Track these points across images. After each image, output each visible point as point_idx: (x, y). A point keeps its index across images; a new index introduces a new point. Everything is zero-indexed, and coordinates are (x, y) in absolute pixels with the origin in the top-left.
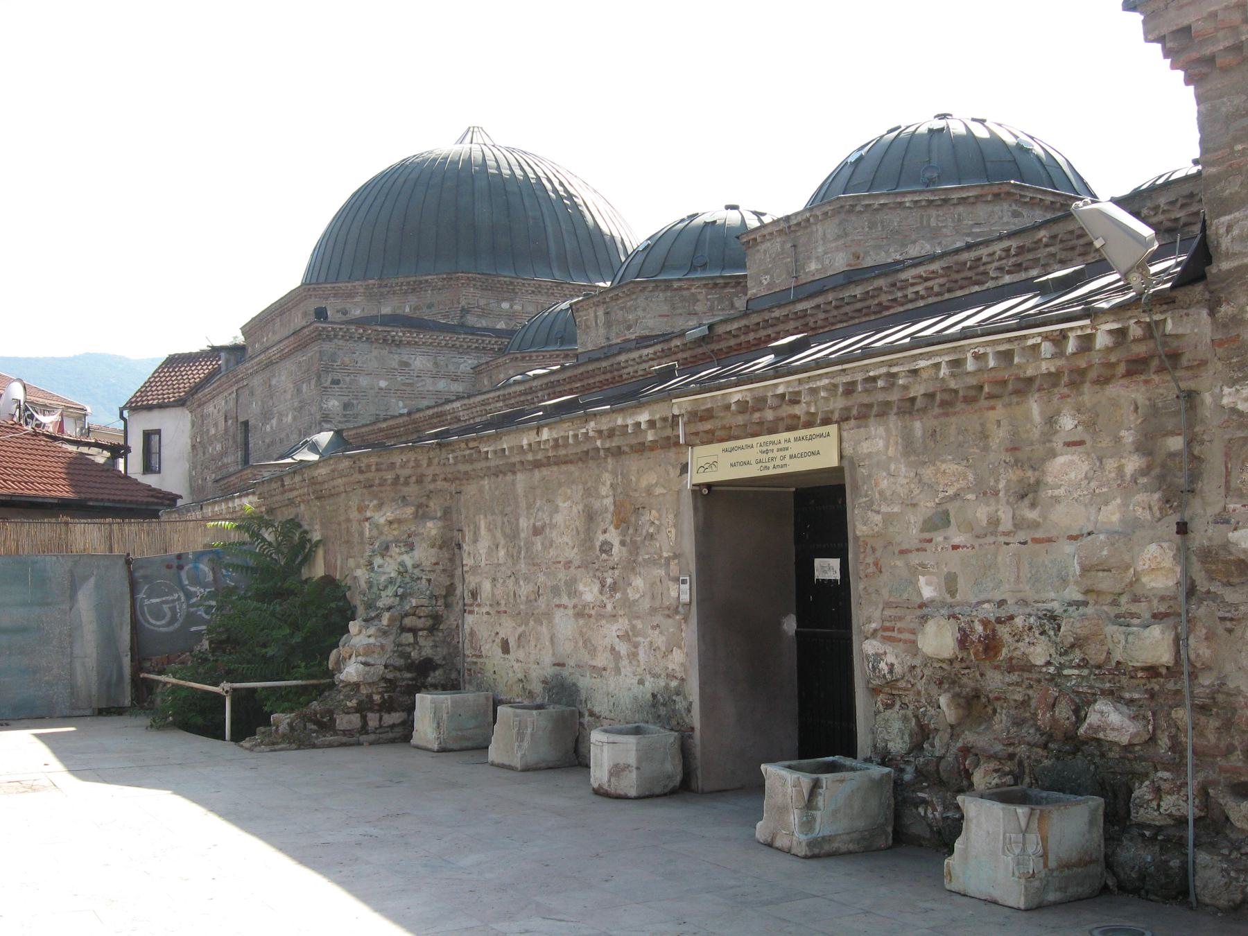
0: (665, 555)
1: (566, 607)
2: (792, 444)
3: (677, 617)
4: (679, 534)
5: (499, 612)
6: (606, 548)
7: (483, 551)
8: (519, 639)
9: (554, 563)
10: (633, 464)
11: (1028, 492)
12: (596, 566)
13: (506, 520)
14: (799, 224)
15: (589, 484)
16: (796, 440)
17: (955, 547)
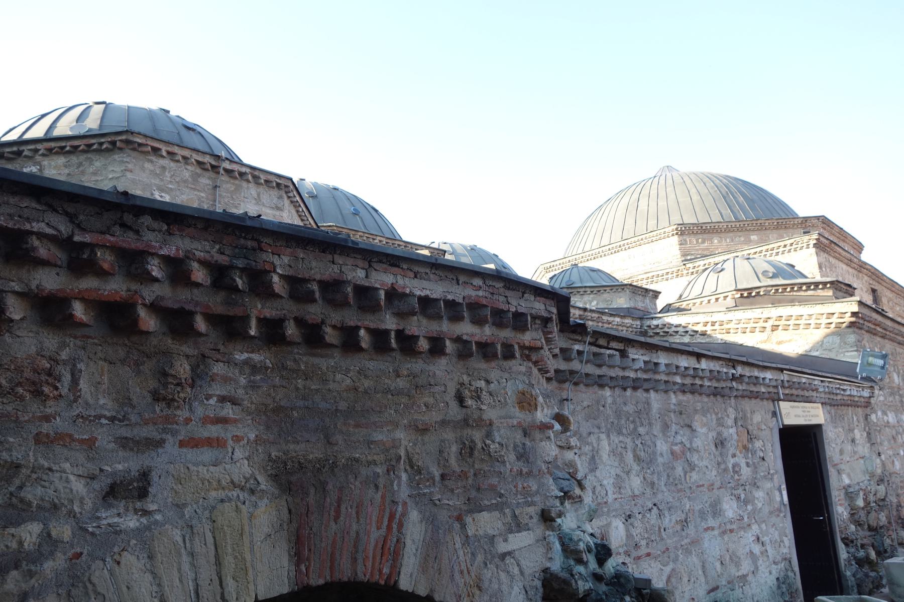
0: (772, 472)
1: (713, 529)
2: (810, 410)
3: (782, 515)
4: (775, 457)
5: (639, 558)
6: (736, 469)
7: (608, 482)
8: (667, 582)
9: (698, 486)
10: (748, 405)
11: (853, 441)
12: (732, 485)
13: (638, 442)
14: (227, 171)
15: (720, 415)
16: (812, 408)
17: (848, 462)
